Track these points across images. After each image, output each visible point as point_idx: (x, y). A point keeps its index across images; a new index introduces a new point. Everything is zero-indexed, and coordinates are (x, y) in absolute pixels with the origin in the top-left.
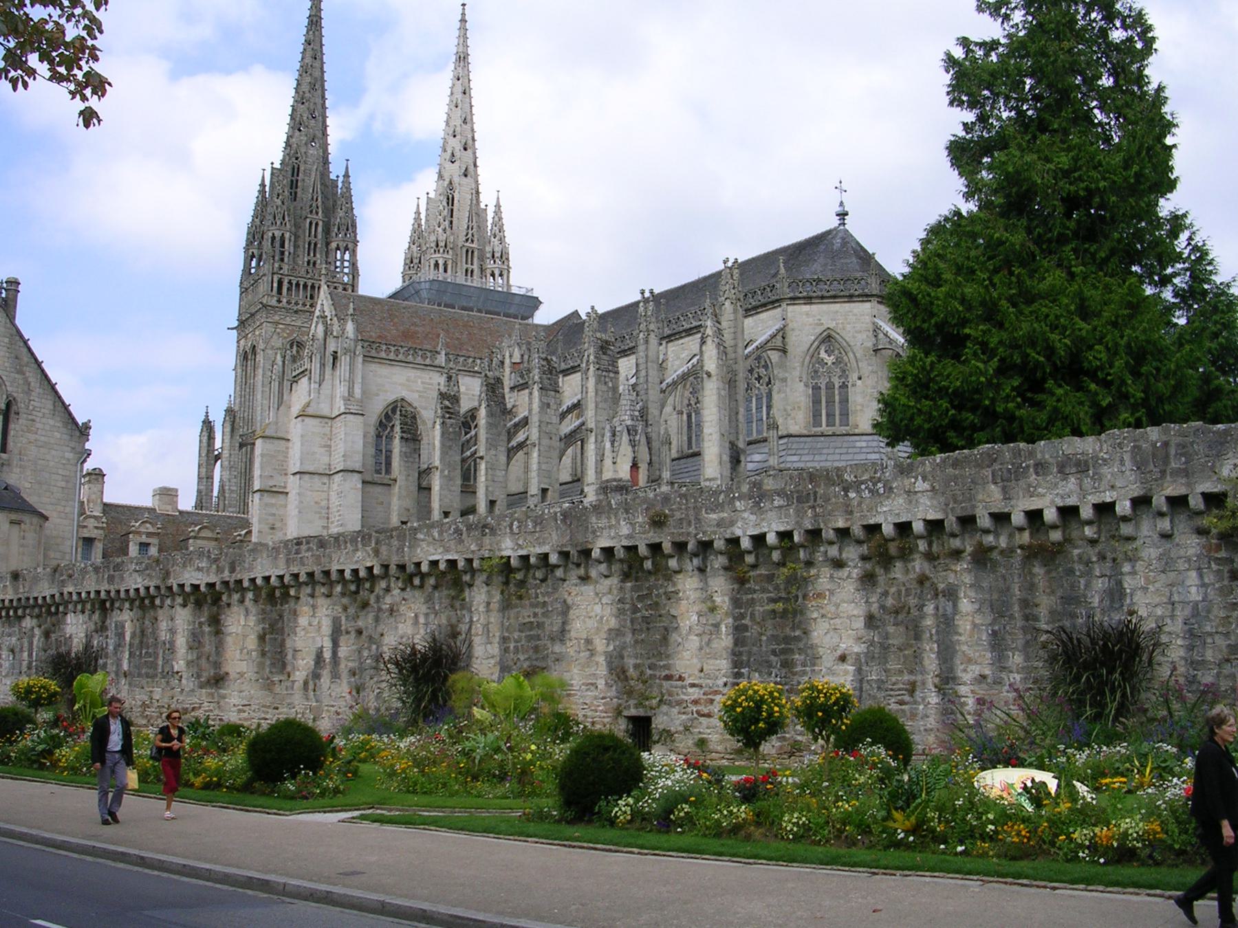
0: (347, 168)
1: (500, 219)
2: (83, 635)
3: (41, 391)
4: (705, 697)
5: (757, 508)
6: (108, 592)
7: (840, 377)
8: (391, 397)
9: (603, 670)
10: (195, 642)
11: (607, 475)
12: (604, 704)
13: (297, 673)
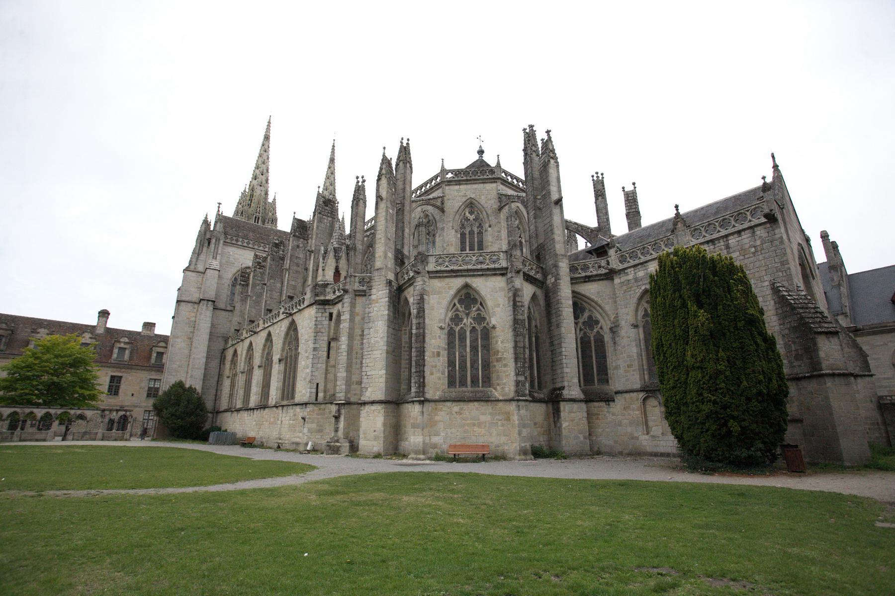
7: (478, 227)
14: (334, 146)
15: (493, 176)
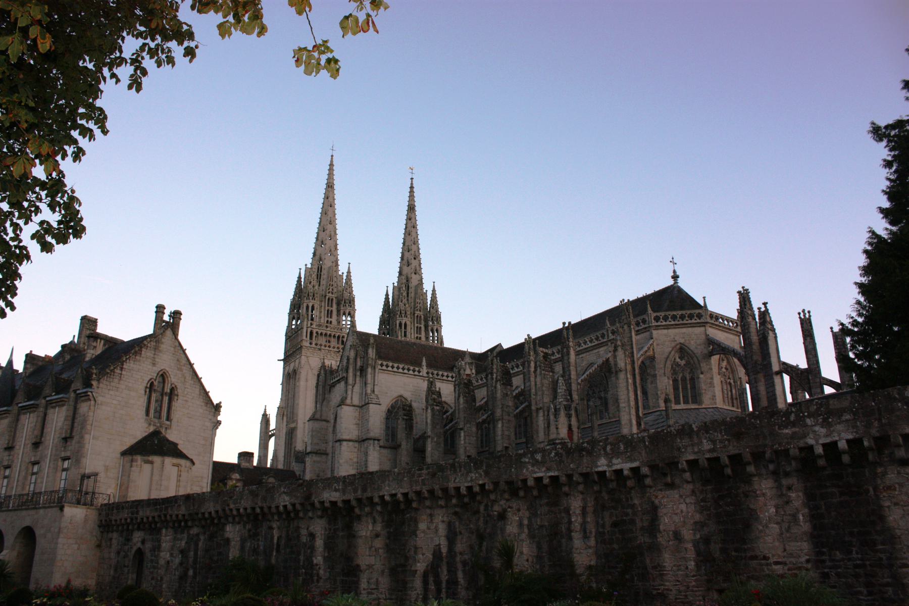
0: (349, 268)
1: (436, 298)
2: (238, 539)
3: (192, 382)
4: (790, 572)
5: (826, 423)
6: (262, 508)
8: (396, 395)
9: (691, 554)
10: (329, 545)
11: (552, 436)
12: (695, 581)
13: (418, 564)
14: (412, 187)
15: (702, 320)
